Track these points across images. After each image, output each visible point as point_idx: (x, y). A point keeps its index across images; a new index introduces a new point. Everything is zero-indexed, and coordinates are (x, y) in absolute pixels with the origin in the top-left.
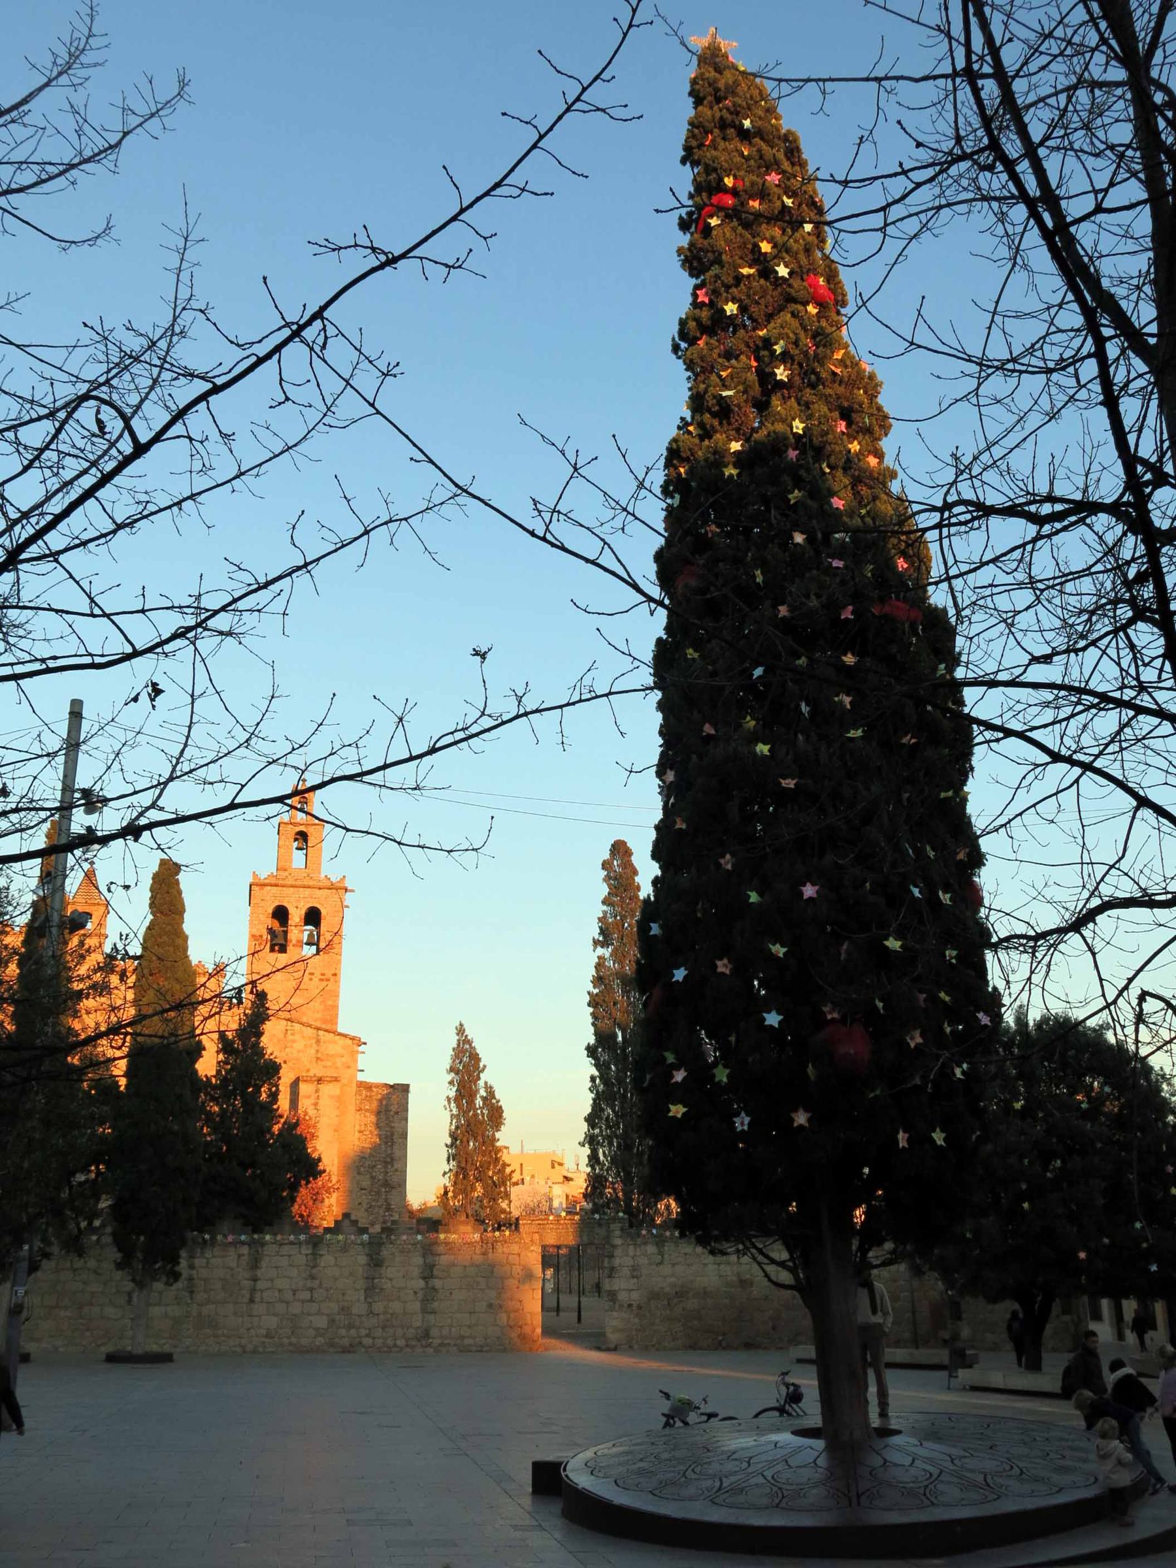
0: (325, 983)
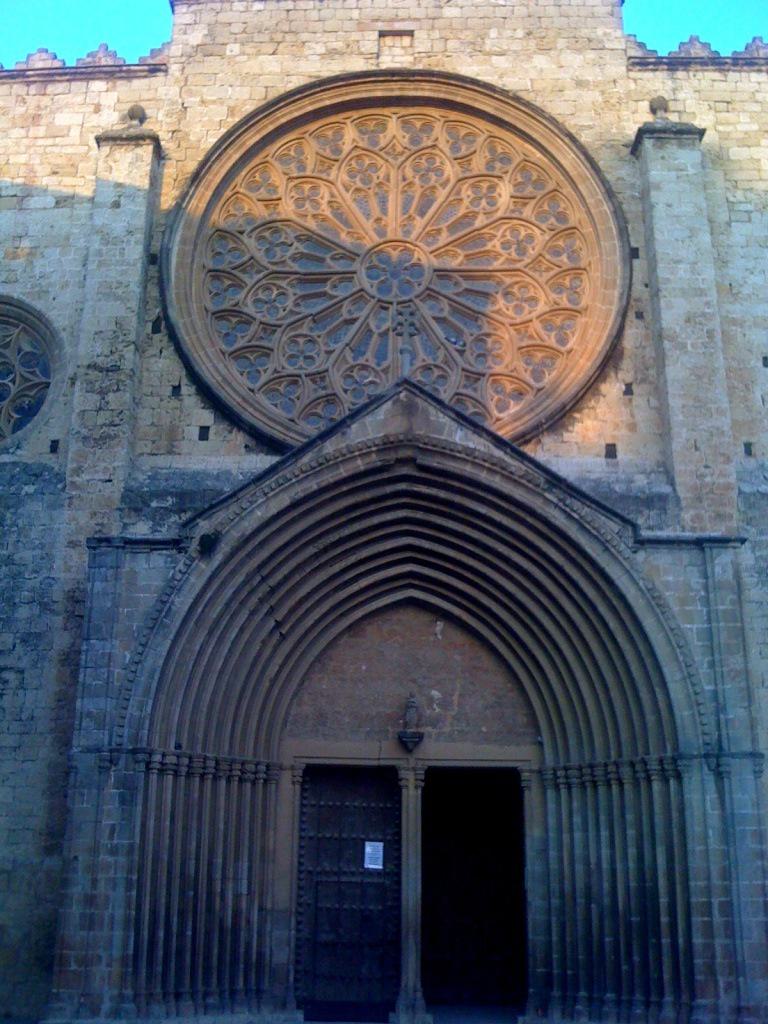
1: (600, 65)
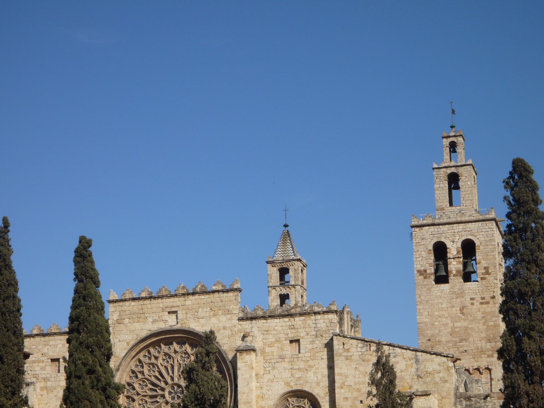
0: (485, 306)
1: (230, 319)
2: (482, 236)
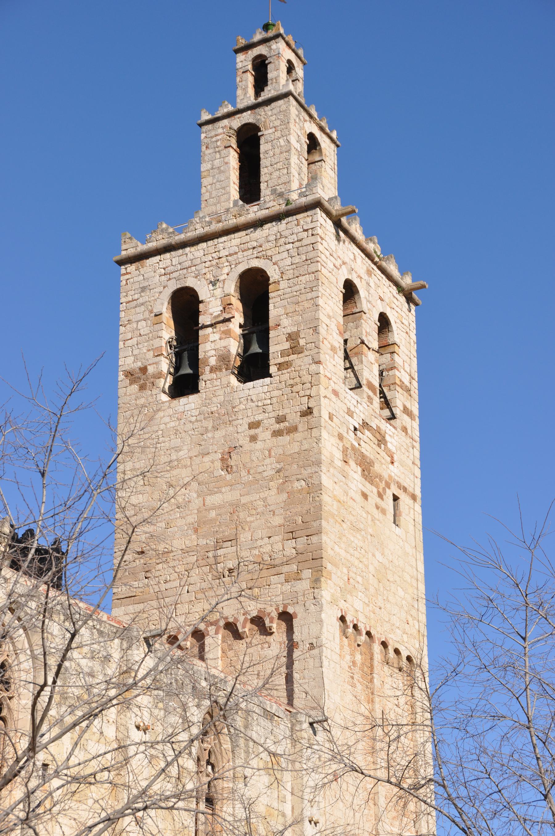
0: (286, 438)
2: (285, 254)
